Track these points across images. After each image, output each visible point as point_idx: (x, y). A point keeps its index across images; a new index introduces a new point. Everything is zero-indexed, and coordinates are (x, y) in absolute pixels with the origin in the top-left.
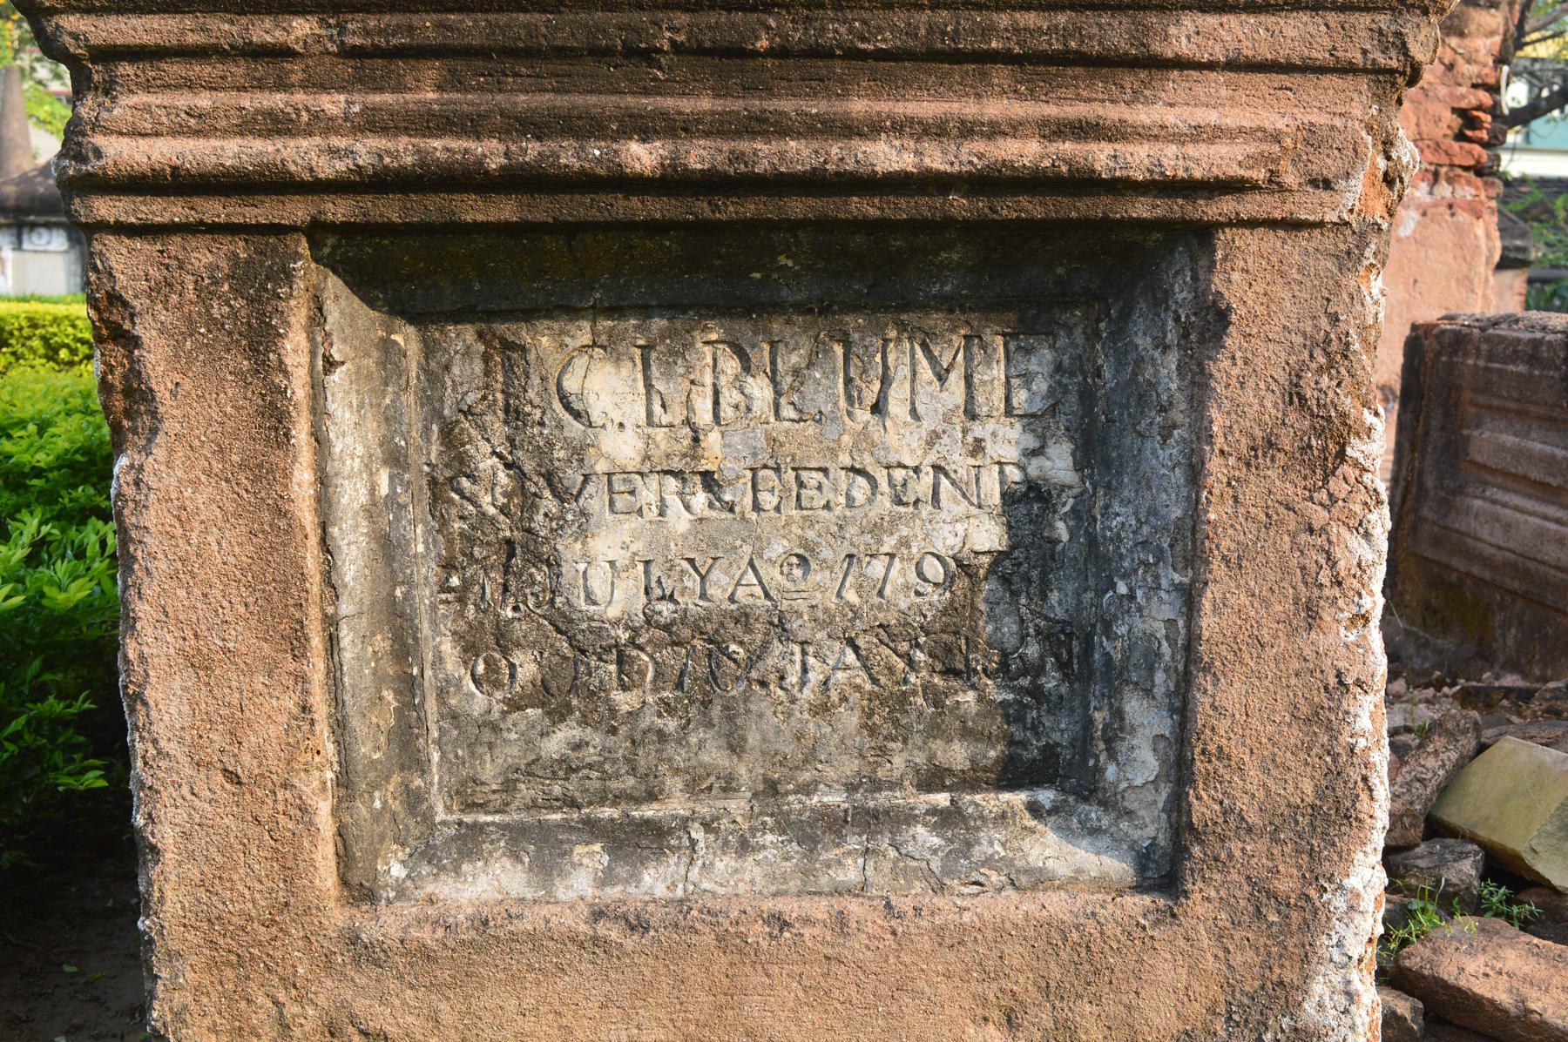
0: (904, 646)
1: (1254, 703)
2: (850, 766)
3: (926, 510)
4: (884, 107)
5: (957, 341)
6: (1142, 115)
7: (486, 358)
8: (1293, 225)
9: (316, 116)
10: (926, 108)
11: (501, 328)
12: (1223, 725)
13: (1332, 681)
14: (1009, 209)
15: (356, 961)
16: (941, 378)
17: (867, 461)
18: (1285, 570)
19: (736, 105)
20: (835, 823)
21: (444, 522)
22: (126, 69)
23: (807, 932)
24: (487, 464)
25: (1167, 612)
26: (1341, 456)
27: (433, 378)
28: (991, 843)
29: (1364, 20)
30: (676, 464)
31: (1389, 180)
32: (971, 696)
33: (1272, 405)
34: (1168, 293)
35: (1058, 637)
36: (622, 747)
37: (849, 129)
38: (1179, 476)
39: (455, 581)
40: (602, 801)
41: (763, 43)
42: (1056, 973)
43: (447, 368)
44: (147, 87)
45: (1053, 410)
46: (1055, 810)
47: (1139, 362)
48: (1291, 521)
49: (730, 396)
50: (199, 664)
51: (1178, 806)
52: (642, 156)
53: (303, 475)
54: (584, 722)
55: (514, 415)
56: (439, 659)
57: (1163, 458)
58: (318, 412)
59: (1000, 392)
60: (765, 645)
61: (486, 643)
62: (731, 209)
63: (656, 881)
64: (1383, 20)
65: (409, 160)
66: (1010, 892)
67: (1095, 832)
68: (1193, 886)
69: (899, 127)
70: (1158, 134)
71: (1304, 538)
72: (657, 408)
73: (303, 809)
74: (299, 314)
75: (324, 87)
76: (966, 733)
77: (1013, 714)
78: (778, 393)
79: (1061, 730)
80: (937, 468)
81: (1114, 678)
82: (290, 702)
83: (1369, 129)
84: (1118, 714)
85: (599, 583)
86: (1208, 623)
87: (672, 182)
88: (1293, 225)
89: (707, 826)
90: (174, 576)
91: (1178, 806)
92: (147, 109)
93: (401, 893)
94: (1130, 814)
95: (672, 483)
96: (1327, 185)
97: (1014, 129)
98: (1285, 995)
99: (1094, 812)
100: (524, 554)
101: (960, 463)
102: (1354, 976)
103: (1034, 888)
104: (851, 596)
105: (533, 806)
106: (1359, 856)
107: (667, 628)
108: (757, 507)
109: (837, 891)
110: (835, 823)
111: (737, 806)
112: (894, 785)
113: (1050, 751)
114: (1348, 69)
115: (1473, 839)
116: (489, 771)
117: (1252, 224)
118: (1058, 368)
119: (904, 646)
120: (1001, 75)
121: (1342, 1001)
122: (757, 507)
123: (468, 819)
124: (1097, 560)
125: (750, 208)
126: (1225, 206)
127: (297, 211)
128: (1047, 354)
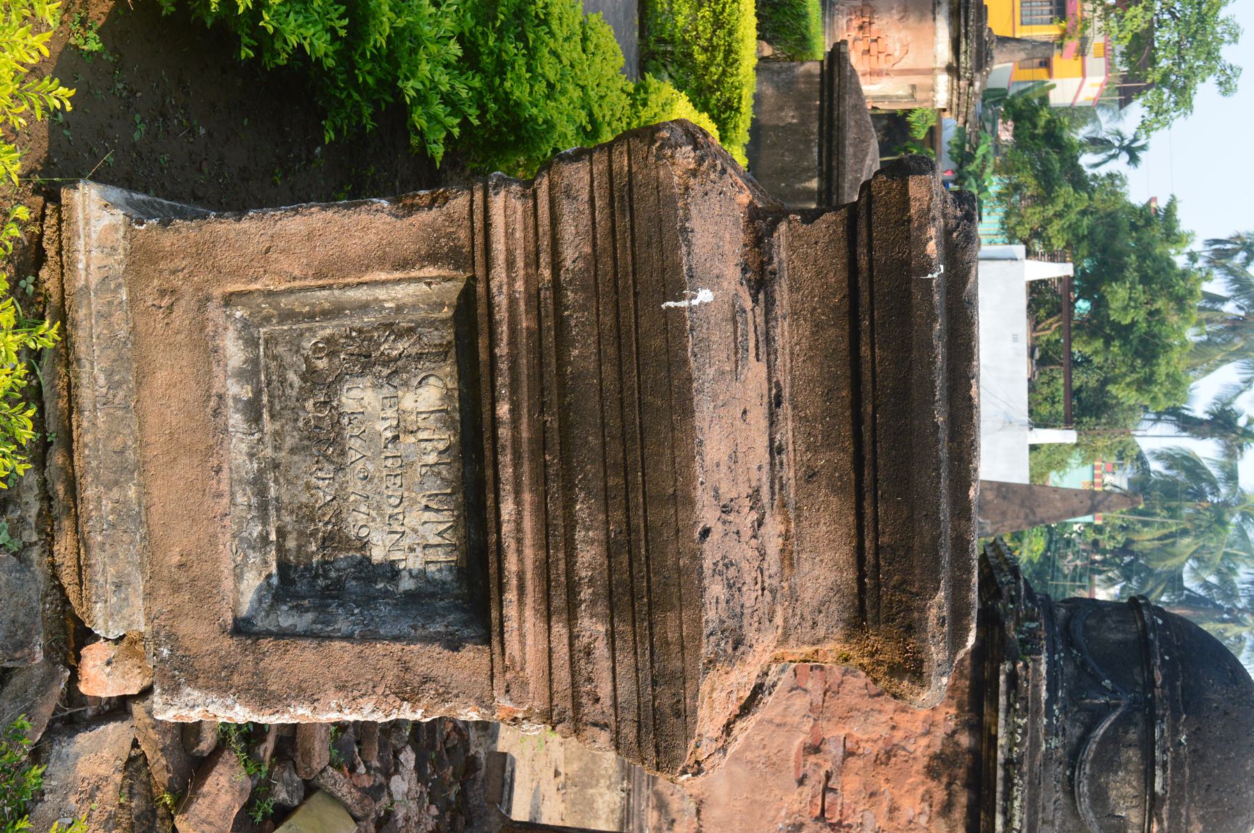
0: (333, 520)
1: (307, 664)
2: (285, 499)
3: (387, 528)
4: (527, 507)
5: (454, 541)
6: (529, 613)
7: (441, 345)
8: (492, 677)
9: (514, 280)
10: (528, 524)
11: (453, 351)
12: (297, 652)
13: (315, 697)
14: (492, 558)
15: (199, 301)
16: (440, 534)
17: (405, 504)
18: (358, 677)
19: (525, 447)
20: (262, 492)
21: (377, 329)
22: (531, 203)
23: (214, 482)
24: (400, 346)
25: (344, 629)
26: (404, 699)
27: (432, 323)
28: (254, 558)
29: (569, 705)
30: (402, 424)
31: (515, 720)
32: (314, 548)
33: (421, 670)
34: (468, 627)
35: (338, 584)
36: (291, 404)
37: (517, 493)
38: (396, 632)
39: (354, 334)
40: (270, 396)
41: (548, 458)
42: (200, 584)
43: (437, 329)
44: (525, 211)
45: (428, 581)
46: (269, 584)
47: (444, 616)
48: (377, 679)
49: (429, 446)
50: (310, 236)
51: (268, 634)
52: (503, 410)
53: (383, 276)
54: (301, 388)
55: (420, 357)
56: (324, 328)
57: (404, 627)
58: (410, 280)
59: (434, 559)
60: (332, 462)
61: (331, 347)
62: (487, 445)
63: (236, 420)
64: (570, 713)
65: (497, 317)
66: (233, 565)
67: (260, 601)
68: (234, 641)
69: (519, 513)
70: (521, 620)
71: (371, 684)
72: (424, 416)
73: (257, 279)
74: (444, 272)
75: (526, 282)
76: (299, 547)
77: (308, 568)
78: (431, 466)
79: (302, 587)
80: (403, 533)
81: (321, 608)
82: (297, 273)
83: (530, 709)
84: (307, 610)
85: (354, 393)
86: (337, 645)
87: (495, 422)
88: (492, 677)
89: (260, 440)
90: (343, 226)
91: (268, 634)
92: (515, 213)
93: (228, 317)
94: (268, 616)
95: (395, 423)
96: (507, 691)
97: (521, 561)
98: (193, 680)
99: (268, 601)
100: (366, 362)
101: (406, 542)
102: (200, 709)
103: (235, 575)
104: (352, 498)
105: (267, 368)
106: (248, 710)
107: (338, 421)
108: (387, 458)
109: (233, 494)
110: (262, 492)
111: (269, 452)
112: (278, 517)
113: (293, 582)
114: (551, 700)
115: (301, 803)
116: (280, 349)
117: (492, 660)
118: (444, 583)
119: (333, 520)
120: (542, 554)
121: (191, 704)
122: (387, 458)
123: (261, 341)
124: (368, 601)
125: (488, 453)
126: (497, 649)
127: (480, 273)
128: (450, 578)
